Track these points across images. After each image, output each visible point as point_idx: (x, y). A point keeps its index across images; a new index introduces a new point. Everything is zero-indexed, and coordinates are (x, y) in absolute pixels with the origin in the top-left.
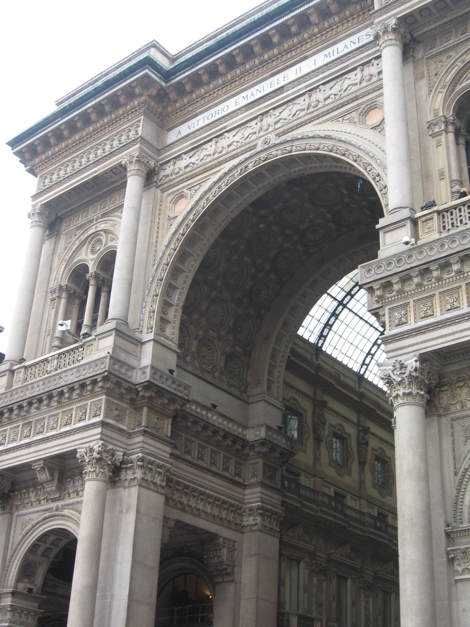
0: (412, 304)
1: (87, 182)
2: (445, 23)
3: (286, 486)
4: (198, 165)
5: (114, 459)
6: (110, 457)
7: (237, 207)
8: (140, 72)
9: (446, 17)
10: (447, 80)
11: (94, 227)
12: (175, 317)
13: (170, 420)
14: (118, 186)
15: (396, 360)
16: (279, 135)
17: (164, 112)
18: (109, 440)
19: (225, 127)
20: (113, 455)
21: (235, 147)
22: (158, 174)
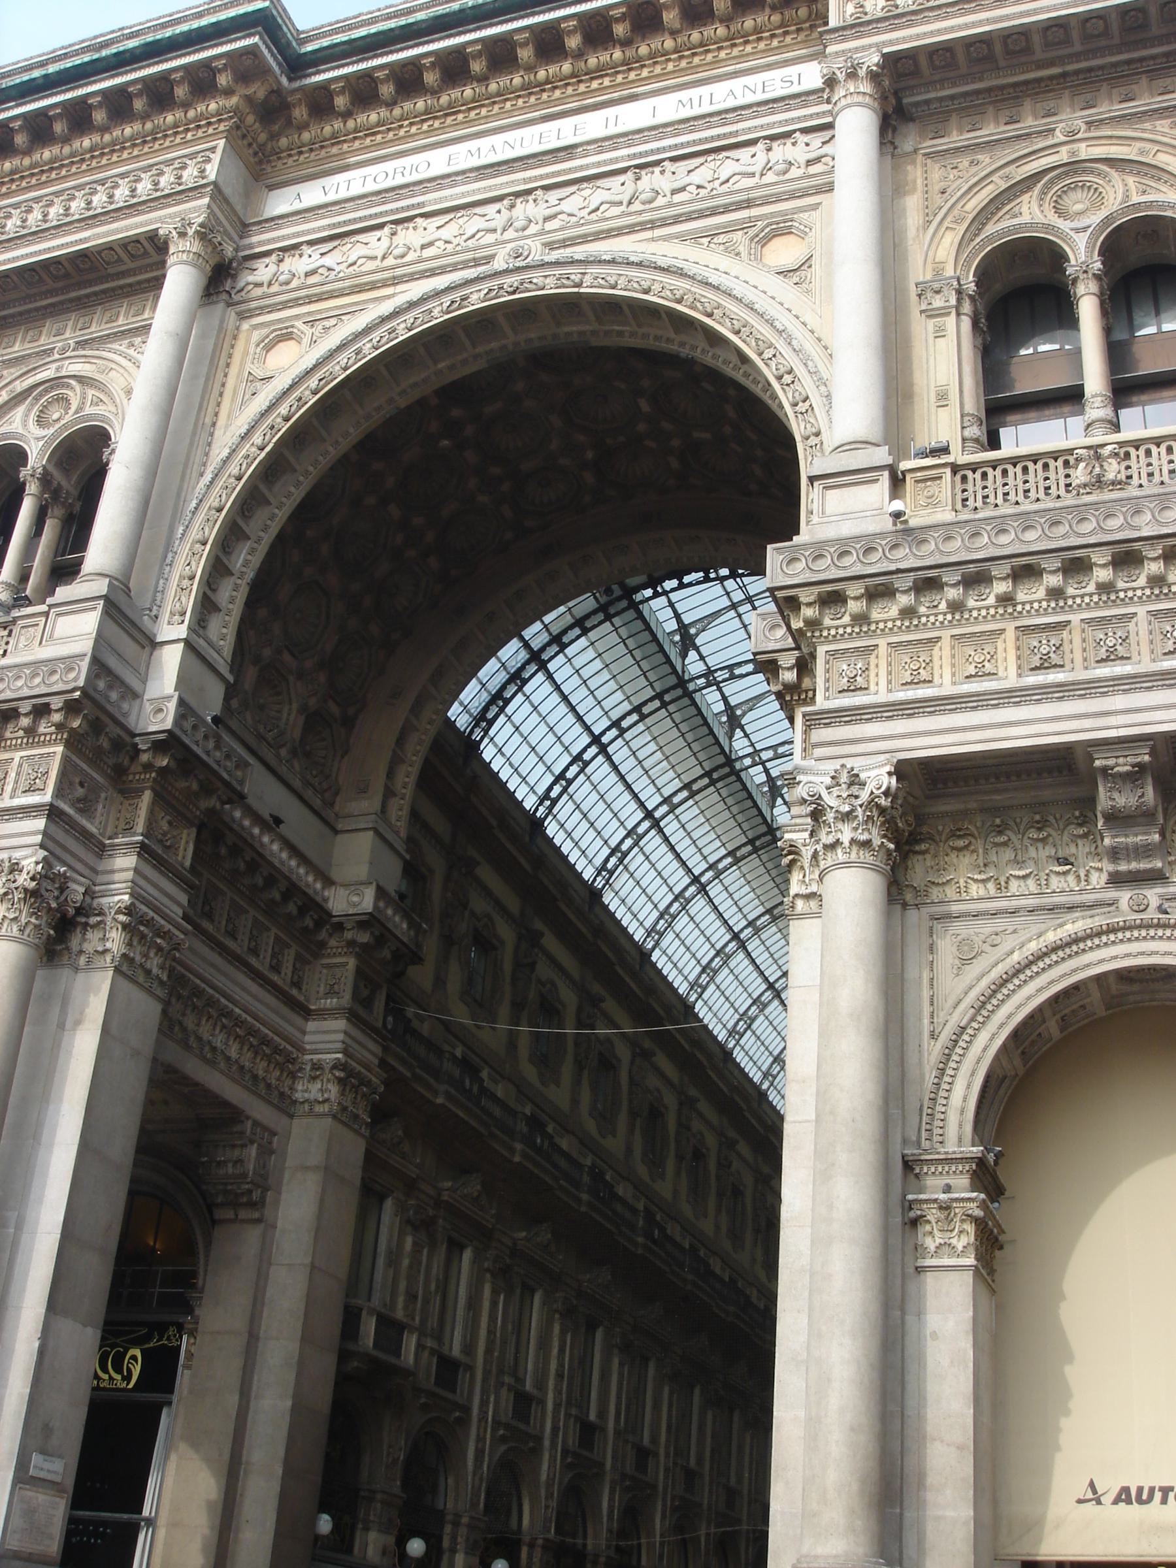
0: (883, 649)
1: (56, 261)
2: (977, 92)
3: (389, 1027)
4: (342, 275)
5: (62, 898)
6: (56, 893)
7: (416, 385)
8: (239, 39)
9: (981, 80)
10: (968, 207)
11: (54, 366)
12: (232, 600)
13: (194, 831)
14: (130, 285)
15: (843, 766)
16: (551, 246)
17: (269, 146)
18: (58, 851)
19: (420, 205)
20: (62, 889)
21: (440, 252)
22: (234, 277)
